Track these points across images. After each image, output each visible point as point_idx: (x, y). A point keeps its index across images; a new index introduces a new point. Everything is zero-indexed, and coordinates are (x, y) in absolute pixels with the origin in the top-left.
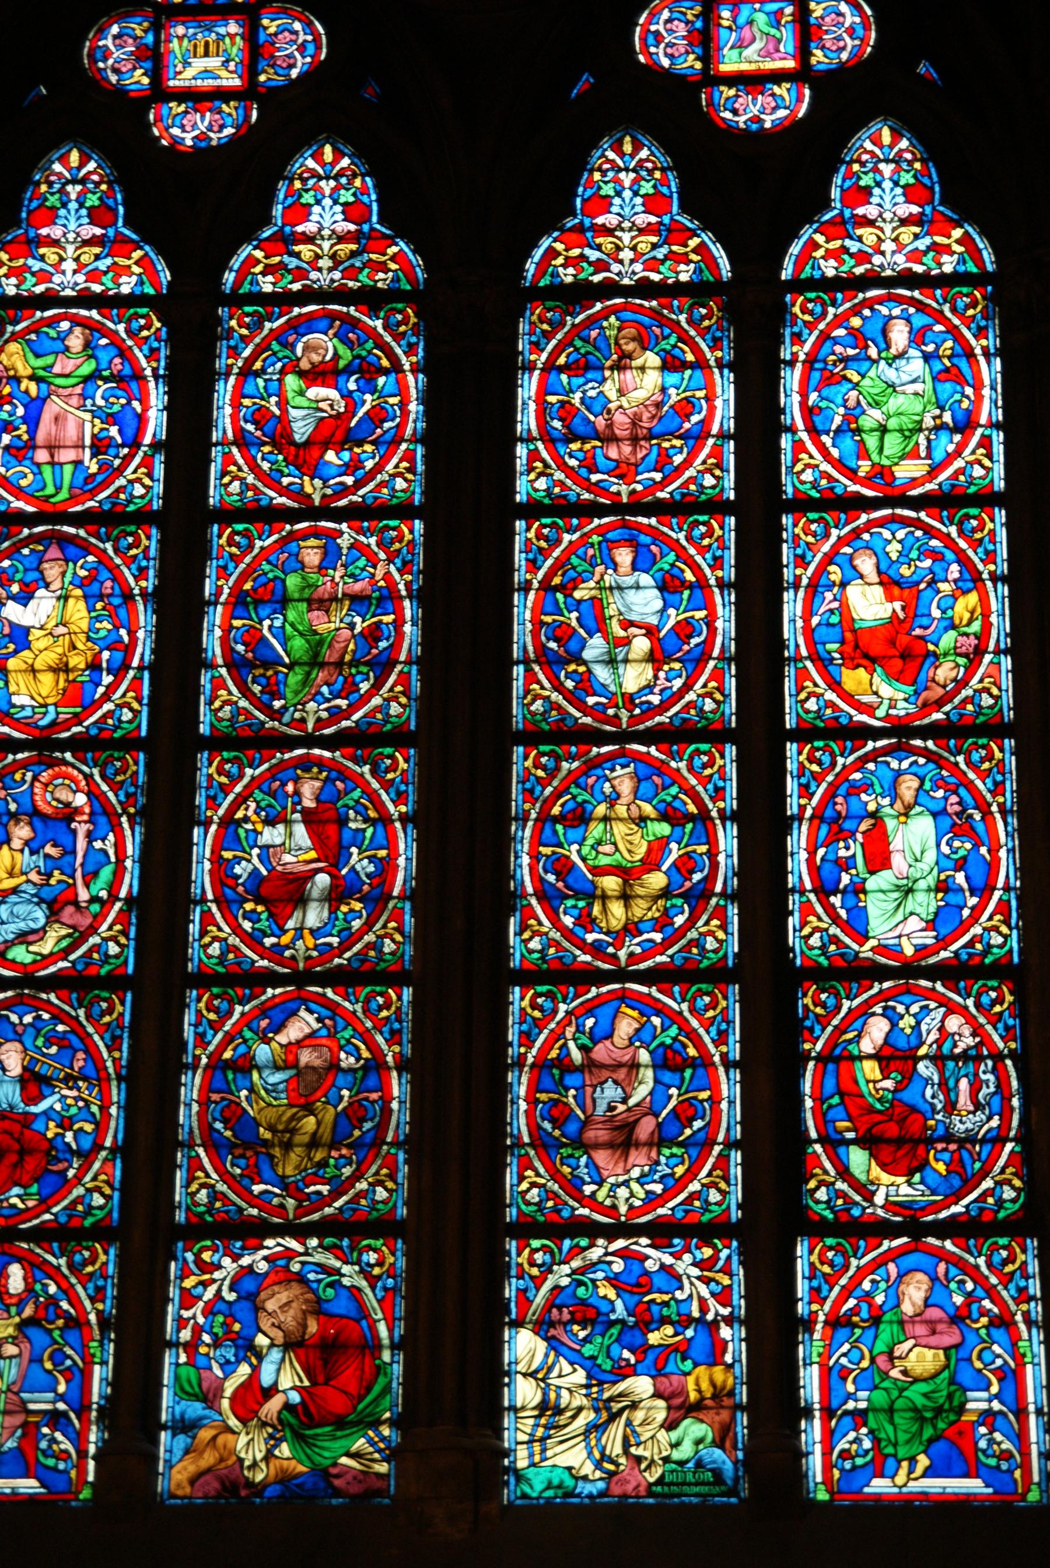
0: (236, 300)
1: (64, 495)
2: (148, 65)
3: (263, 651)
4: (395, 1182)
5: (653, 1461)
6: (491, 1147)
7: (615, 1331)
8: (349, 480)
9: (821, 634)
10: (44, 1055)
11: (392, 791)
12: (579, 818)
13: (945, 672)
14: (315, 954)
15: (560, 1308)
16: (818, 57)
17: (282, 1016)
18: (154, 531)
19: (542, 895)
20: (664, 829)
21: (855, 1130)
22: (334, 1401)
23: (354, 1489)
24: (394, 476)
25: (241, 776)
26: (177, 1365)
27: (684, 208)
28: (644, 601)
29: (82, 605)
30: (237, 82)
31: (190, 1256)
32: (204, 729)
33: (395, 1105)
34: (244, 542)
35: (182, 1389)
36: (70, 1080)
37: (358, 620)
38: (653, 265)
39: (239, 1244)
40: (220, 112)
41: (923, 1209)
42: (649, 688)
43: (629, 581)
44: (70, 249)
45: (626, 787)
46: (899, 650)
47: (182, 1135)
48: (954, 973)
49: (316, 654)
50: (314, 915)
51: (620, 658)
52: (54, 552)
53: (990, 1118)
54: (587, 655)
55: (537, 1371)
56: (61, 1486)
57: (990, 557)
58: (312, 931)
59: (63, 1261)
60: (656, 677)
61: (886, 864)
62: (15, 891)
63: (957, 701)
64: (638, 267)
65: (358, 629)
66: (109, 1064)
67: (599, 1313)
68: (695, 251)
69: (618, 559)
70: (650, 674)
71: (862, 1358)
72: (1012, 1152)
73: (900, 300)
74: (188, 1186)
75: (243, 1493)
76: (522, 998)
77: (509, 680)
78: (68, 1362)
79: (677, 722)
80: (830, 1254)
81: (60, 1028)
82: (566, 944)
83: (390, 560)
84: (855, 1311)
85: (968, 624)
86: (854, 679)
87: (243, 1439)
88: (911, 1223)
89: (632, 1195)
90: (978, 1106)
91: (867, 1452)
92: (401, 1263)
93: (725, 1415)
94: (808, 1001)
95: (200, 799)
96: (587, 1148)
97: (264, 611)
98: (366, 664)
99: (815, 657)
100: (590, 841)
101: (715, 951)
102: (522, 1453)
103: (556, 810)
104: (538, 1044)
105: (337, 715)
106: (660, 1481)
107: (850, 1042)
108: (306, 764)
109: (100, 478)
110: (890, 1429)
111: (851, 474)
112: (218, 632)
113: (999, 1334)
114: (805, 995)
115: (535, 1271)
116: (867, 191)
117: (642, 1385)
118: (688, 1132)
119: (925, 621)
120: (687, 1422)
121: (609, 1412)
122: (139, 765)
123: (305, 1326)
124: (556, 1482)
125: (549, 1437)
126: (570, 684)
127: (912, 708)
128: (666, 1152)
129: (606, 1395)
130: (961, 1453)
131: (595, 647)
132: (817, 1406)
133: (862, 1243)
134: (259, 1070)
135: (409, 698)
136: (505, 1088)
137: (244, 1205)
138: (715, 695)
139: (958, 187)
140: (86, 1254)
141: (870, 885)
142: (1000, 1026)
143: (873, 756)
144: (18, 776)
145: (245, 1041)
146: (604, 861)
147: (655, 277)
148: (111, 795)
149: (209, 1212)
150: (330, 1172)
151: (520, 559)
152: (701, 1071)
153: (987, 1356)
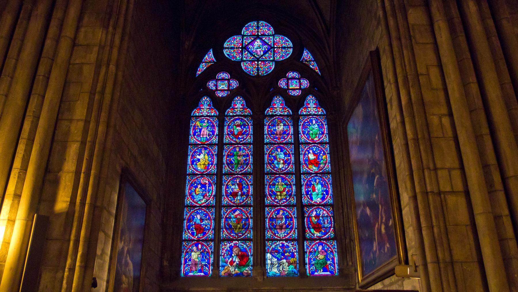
0: (227, 116)
6: (264, 229)
12: (274, 185)
20: (286, 186)
22: (243, 263)
28: (282, 156)
36: (206, 220)
38: (282, 112)
45: (280, 181)
46: (316, 163)
48: (325, 205)
50: (239, 198)
52: (203, 149)
57: (327, 151)
61: (315, 191)
86: (310, 166)
88: (320, 238)
96: (276, 229)
102: (269, 270)
105: (241, 171)
111: (309, 140)
121: (280, 265)
122: (215, 177)
131: (276, 162)
138: (291, 168)
139: (321, 103)
151: (265, 150)
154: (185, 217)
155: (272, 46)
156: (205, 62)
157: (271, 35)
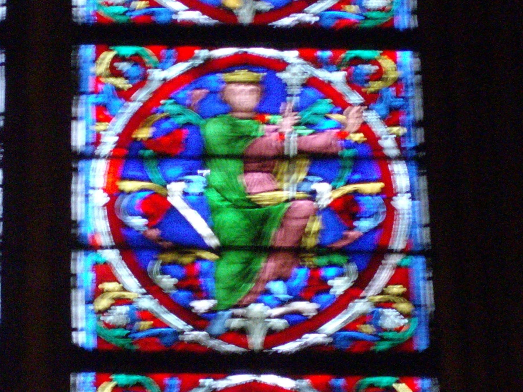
98: (342, 251)
112: (101, 198)
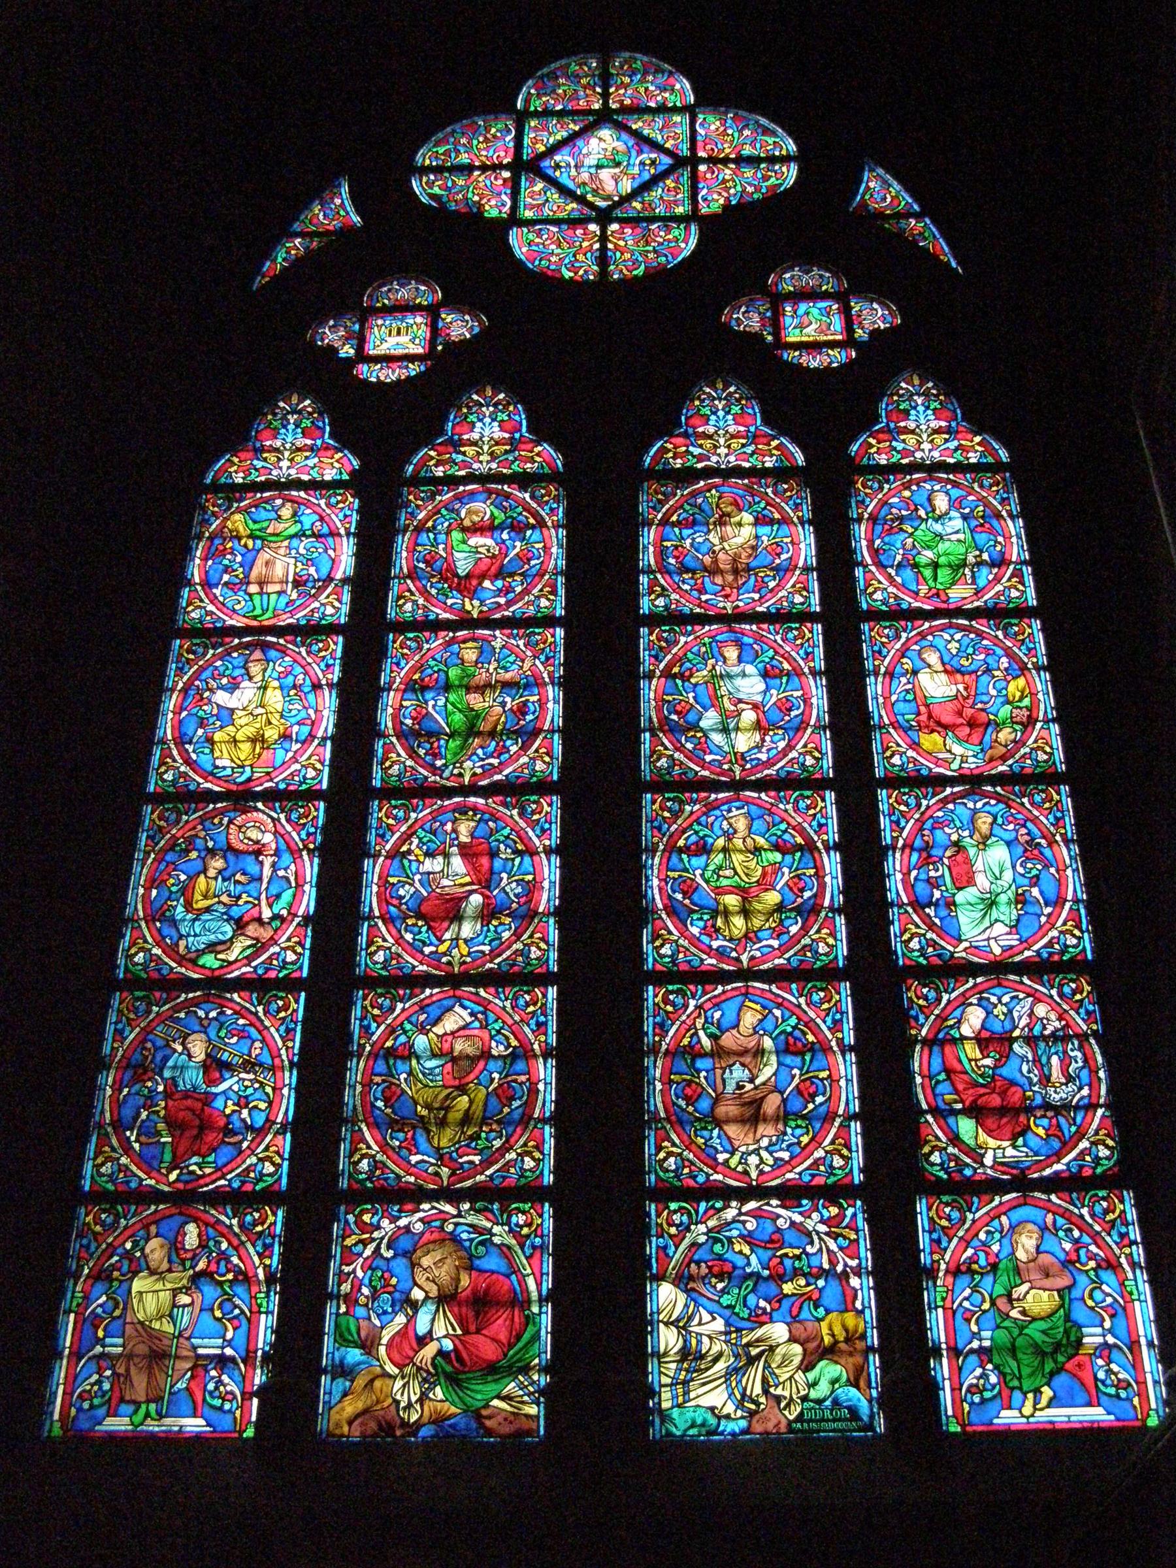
0: (416, 481)
1: (269, 614)
2: (355, 342)
3: (428, 724)
4: (542, 1153)
5: (791, 1399)
7: (750, 1283)
8: (502, 600)
9: (900, 707)
10: (226, 1044)
11: (538, 828)
12: (702, 849)
13: (1005, 735)
14: (469, 959)
15: (698, 1263)
16: (859, 332)
17: (438, 1012)
18: (341, 639)
19: (671, 910)
20: (777, 857)
21: (962, 1101)
23: (506, 1429)
24: (538, 597)
25: (406, 819)
26: (338, 1314)
27: (766, 421)
28: (751, 685)
29: (278, 692)
30: (421, 351)
31: (351, 1218)
32: (377, 783)
33: (541, 1086)
34: (414, 645)
35: (341, 1336)
36: (250, 1065)
37: (508, 699)
39: (396, 1208)
40: (407, 367)
41: (1029, 1168)
42: (758, 747)
43: (736, 670)
44: (287, 454)
45: (741, 824)
47: (348, 1112)
48: (1038, 968)
49: (473, 726)
50: (468, 929)
51: (731, 726)
52: (258, 654)
53: (1080, 1089)
54: (702, 724)
55: (678, 1320)
56: (226, 1423)
57: (1031, 652)
58: (466, 941)
59: (235, 1221)
60: (763, 740)
61: (971, 882)
62: (208, 910)
63: (1017, 757)
64: (732, 458)
65: (508, 706)
66: (283, 1052)
67: (735, 1267)
68: (776, 448)
69: (727, 655)
70: (758, 738)
71: (983, 1301)
72: (1103, 1116)
73: (940, 480)
74: (351, 1155)
75: (398, 1433)
76: (656, 996)
77: (638, 742)
78: (237, 1311)
79: (783, 774)
80: (947, 1210)
81: (241, 1022)
82: (693, 949)
83: (535, 657)
84: (973, 1260)
85: (1021, 699)
86: (930, 741)
87: (399, 1384)
88: (1020, 1182)
89: (762, 1161)
90: (1070, 1079)
91: (994, 1387)
92: (549, 1224)
93: (859, 1359)
94: (911, 994)
95: (372, 837)
96: (719, 1123)
97: (429, 695)
99: (895, 725)
100: (712, 867)
101: (826, 954)
102: (666, 1395)
103: (681, 843)
104: (671, 1033)
106: (800, 1418)
107: (952, 1027)
108: (462, 810)
109: (298, 603)
110: (1014, 1364)
112: (390, 710)
113: (1108, 1276)
114: (908, 989)
115: (673, 1230)
116: (907, 413)
117: (778, 1331)
118: (811, 1106)
119: (985, 698)
120: (823, 1363)
123: (458, 1280)
124: (699, 1421)
125: (692, 1380)
126: (689, 746)
127: (980, 763)
128: (793, 1124)
129: (744, 1341)
130: (1083, 1384)
131: (710, 719)
132: (944, 1346)
133: (975, 1200)
134: (418, 1058)
135: (551, 758)
136: (643, 1071)
137: (402, 1173)
140: (257, 1215)
141: (960, 898)
142: (1082, 1011)
143: (953, 798)
144: (216, 821)
145: (405, 1032)
146: (724, 882)
147: (746, 465)
148: (294, 834)
149: (369, 1179)
150: (481, 1144)
151: (644, 655)
152: (820, 1056)
153: (1098, 1295)
154: (107, 1049)
155: (685, 151)
156: (302, 235)
157: (675, 110)
